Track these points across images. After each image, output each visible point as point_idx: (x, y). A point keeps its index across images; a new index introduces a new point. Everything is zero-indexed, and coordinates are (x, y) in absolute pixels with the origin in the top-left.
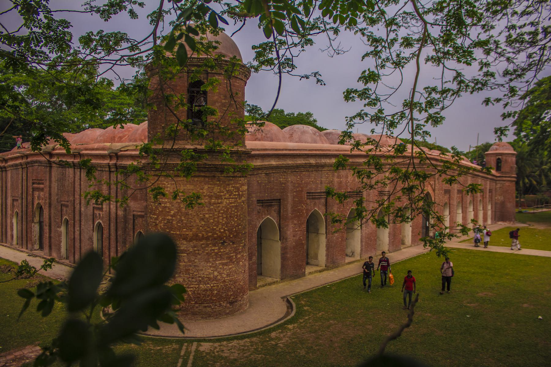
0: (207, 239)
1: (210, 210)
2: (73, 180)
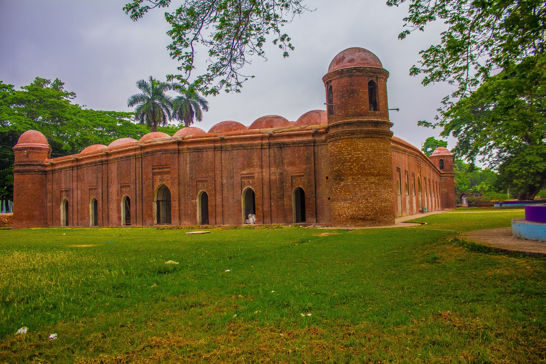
0: (384, 175)
1: (384, 158)
2: (212, 160)
